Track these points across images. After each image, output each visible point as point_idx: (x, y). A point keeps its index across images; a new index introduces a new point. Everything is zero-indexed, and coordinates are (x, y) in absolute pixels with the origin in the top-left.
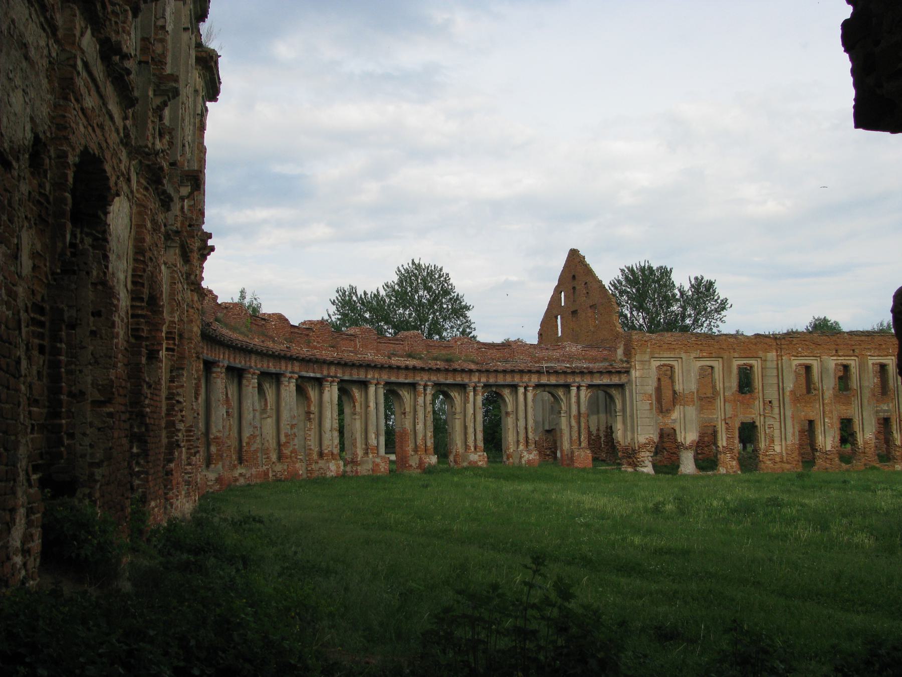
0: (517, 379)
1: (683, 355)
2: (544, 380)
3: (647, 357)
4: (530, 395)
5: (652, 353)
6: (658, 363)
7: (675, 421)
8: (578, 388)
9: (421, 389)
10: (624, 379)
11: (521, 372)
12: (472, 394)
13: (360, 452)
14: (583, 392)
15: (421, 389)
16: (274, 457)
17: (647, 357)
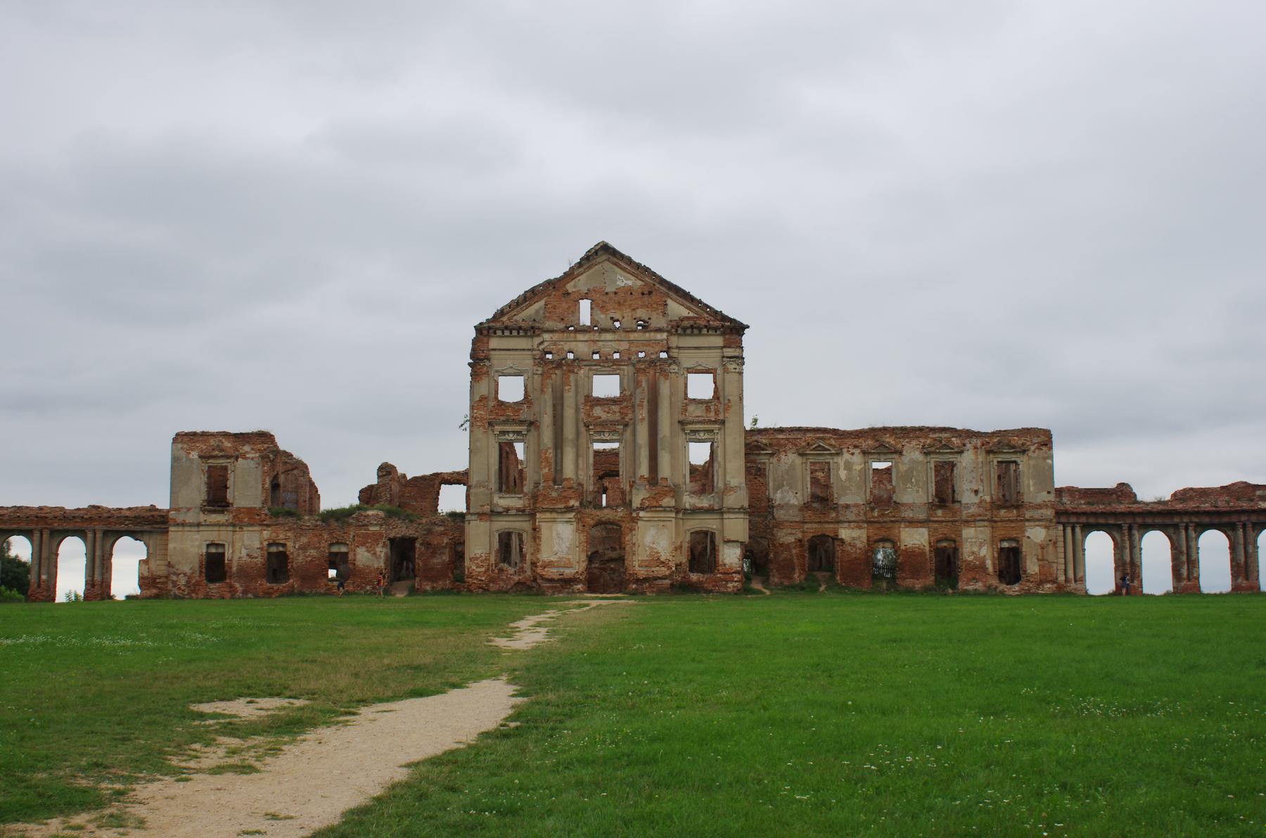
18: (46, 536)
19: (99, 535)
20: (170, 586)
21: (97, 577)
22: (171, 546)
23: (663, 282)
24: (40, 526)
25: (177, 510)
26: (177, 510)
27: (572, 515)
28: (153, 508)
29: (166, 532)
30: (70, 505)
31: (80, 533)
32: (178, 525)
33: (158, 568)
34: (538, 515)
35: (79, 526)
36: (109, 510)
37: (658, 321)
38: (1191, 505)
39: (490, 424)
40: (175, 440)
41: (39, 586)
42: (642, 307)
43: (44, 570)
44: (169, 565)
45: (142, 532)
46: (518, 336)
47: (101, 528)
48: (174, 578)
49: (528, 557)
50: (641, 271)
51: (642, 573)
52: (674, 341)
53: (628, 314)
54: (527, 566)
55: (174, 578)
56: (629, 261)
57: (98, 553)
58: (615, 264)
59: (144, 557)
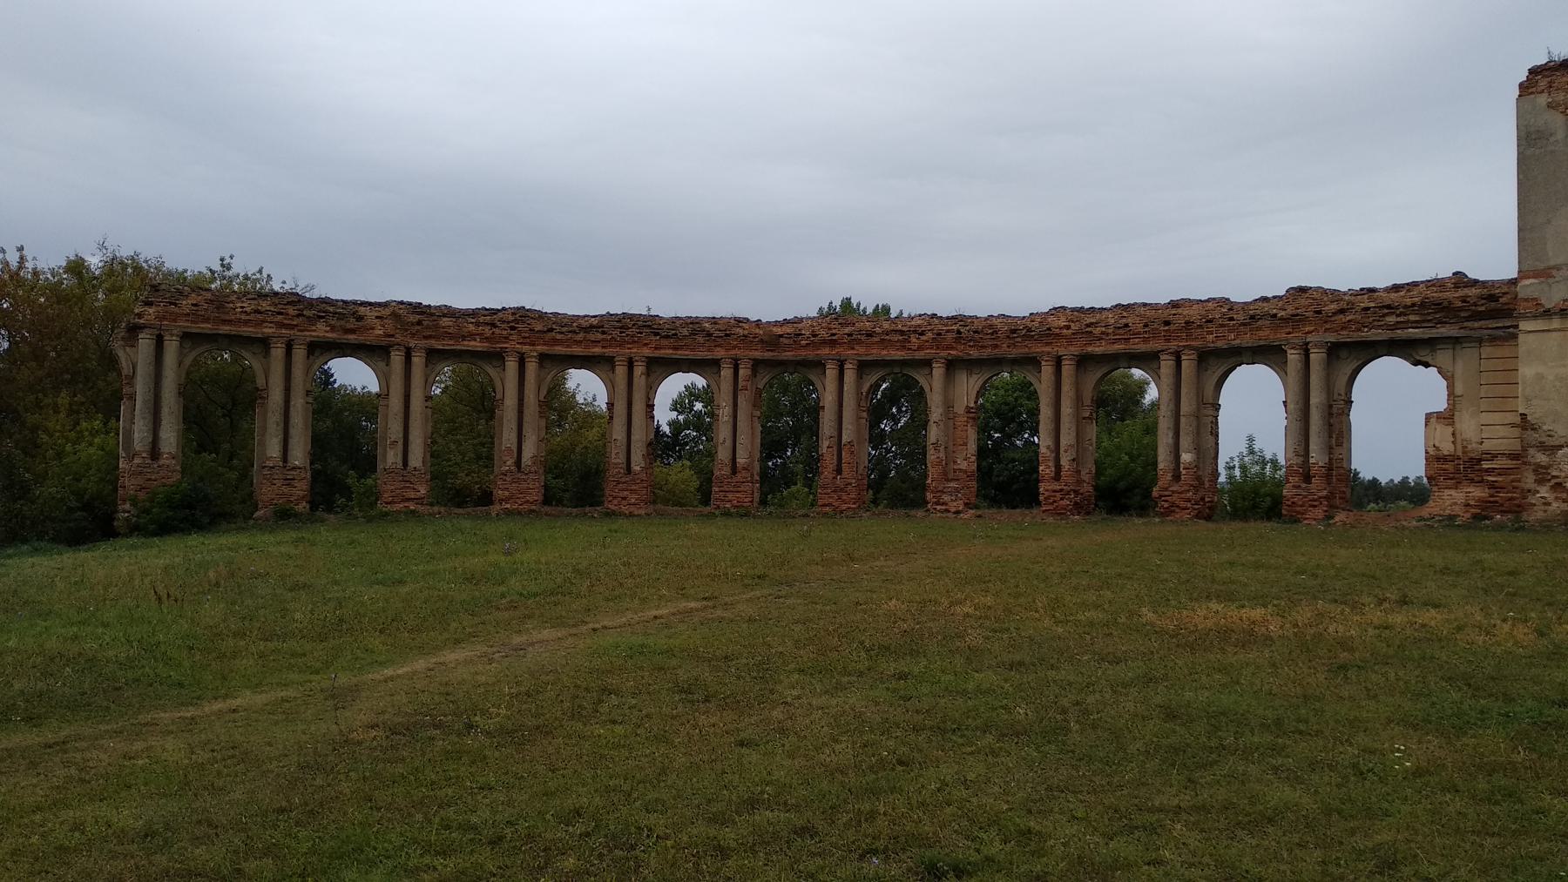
18: (1187, 365)
19: (1317, 357)
20: (1529, 480)
21: (1317, 457)
22: (1527, 371)
24: (1173, 345)
25: (1545, 274)
26: (1545, 274)
28: (1460, 280)
29: (1515, 337)
30: (1243, 293)
31: (1269, 354)
32: (1547, 314)
33: (1486, 431)
35: (1266, 335)
36: (1335, 295)
40: (1525, 89)
41: (1177, 477)
43: (1185, 441)
44: (1525, 423)
45: (1432, 343)
47: (1326, 336)
48: (1542, 458)
55: (1542, 458)
57: (1316, 398)
59: (1441, 404)
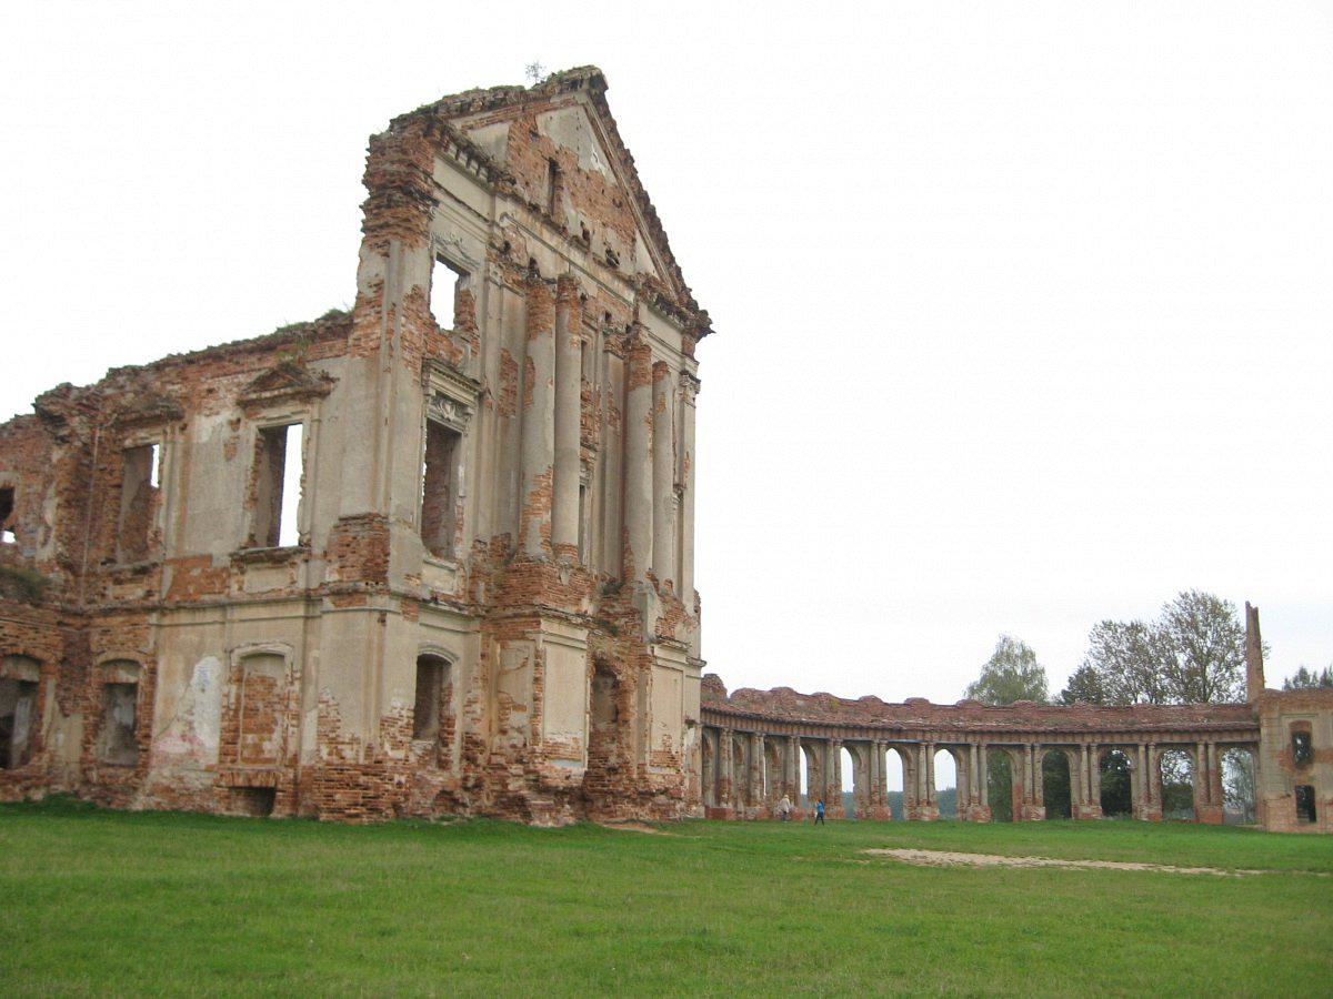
0: (1136, 739)
1: (1319, 711)
2: (1167, 739)
3: (1276, 715)
4: (1152, 753)
5: (1281, 709)
6: (1291, 720)
7: (1312, 778)
8: (1206, 746)
9: (1028, 749)
10: (1256, 737)
11: (1139, 732)
12: (1085, 753)
13: (965, 802)
14: (1211, 750)
15: (1028, 749)
16: (867, 802)
17: (1276, 715)
23: (643, 198)
27: (582, 634)
34: (544, 625)
37: (626, 268)
38: (754, 709)
39: (426, 366)
42: (615, 227)
46: (474, 179)
49: (458, 727)
50: (623, 160)
51: (657, 777)
52: (646, 317)
53: (598, 229)
54: (455, 749)
56: (612, 127)
58: (593, 122)
